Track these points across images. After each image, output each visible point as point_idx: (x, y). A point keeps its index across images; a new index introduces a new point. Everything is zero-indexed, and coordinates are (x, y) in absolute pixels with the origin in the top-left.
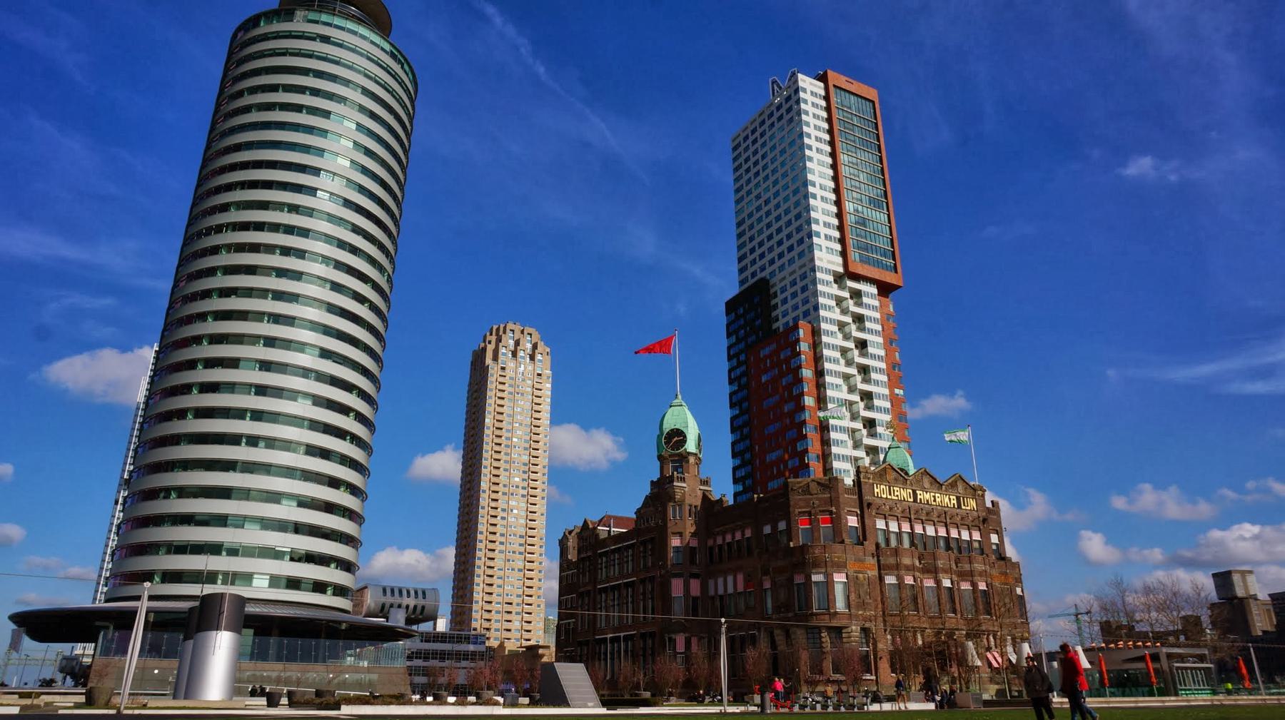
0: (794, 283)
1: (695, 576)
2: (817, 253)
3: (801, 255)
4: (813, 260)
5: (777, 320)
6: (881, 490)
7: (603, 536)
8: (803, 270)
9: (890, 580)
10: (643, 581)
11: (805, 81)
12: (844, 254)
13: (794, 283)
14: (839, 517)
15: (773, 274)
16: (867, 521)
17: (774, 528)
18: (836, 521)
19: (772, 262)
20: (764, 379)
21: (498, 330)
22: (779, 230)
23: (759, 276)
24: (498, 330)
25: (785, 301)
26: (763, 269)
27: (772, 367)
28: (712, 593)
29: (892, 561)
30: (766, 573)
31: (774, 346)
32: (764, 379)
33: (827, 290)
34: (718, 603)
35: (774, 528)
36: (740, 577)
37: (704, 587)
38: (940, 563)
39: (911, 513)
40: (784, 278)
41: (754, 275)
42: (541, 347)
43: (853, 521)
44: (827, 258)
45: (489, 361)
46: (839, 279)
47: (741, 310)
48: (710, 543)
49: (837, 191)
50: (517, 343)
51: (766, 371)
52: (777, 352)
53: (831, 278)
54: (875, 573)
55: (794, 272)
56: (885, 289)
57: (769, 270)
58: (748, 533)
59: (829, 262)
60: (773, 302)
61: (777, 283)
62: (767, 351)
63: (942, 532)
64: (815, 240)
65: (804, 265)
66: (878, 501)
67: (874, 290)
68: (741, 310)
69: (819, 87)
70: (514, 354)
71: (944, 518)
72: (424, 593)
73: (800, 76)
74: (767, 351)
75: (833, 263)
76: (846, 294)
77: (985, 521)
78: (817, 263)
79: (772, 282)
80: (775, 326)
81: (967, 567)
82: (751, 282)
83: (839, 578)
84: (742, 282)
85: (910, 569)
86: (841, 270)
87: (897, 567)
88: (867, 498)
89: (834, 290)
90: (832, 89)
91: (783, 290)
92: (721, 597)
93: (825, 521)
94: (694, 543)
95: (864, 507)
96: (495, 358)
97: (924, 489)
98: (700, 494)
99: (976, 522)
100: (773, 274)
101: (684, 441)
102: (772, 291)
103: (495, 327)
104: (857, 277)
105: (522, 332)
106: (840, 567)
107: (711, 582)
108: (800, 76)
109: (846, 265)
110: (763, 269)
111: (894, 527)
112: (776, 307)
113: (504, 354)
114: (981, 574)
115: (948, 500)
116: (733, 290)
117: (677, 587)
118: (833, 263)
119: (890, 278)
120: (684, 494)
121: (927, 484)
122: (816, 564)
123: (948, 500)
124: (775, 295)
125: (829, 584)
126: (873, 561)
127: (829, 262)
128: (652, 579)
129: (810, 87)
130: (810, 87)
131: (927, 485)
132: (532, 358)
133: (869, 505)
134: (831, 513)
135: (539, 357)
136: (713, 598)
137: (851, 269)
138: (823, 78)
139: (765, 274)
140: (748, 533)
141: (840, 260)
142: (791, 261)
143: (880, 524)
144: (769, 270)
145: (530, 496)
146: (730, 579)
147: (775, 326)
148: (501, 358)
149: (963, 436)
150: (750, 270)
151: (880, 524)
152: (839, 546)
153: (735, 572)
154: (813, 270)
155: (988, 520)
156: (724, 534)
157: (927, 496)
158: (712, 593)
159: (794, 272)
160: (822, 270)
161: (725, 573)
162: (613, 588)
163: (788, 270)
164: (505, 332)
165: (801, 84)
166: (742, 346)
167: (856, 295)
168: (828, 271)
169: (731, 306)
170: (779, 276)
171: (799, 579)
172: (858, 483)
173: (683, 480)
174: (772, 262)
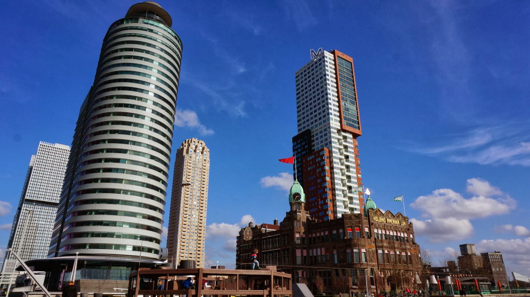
0: (321, 132)
1: (305, 248)
2: (331, 121)
3: (324, 121)
4: (329, 124)
5: (314, 146)
6: (375, 218)
7: (264, 232)
8: (325, 128)
9: (380, 251)
10: (284, 250)
11: (327, 54)
12: (341, 122)
13: (321, 132)
14: (362, 227)
17: (338, 231)
18: (361, 230)
19: (312, 123)
20: (309, 169)
21: (188, 141)
22: (315, 111)
23: (307, 128)
24: (188, 141)
25: (317, 139)
26: (308, 126)
27: (312, 165)
28: (311, 255)
29: (380, 244)
30: (334, 248)
31: (313, 156)
32: (309, 169)
33: (335, 136)
34: (313, 259)
35: (338, 231)
36: (323, 250)
37: (308, 253)
38: (396, 245)
39: (385, 227)
40: (317, 130)
41: (304, 127)
42: (206, 149)
43: (367, 230)
44: (335, 123)
45: (184, 154)
46: (339, 131)
47: (299, 141)
48: (310, 236)
49: (338, 97)
50: (196, 147)
51: (310, 166)
52: (314, 159)
53: (336, 131)
54: (374, 249)
55: (321, 128)
56: (355, 136)
57: (311, 126)
58: (327, 233)
59: (336, 125)
60: (312, 139)
61: (314, 132)
62: (311, 158)
63: (395, 234)
64: (330, 116)
65: (326, 125)
66: (375, 222)
67: (351, 136)
68: (299, 141)
69: (331, 56)
70: (195, 151)
71: (396, 229)
72: (162, 250)
73: (325, 51)
74: (311, 158)
75: (337, 125)
76: (341, 138)
77: (408, 230)
78: (331, 125)
79: (312, 131)
80: (313, 148)
81: (404, 247)
82: (303, 130)
83: (363, 250)
84: (299, 130)
85: (387, 247)
86: (339, 128)
87: (382, 247)
88: (371, 221)
89: (337, 136)
90: (336, 57)
91: (317, 134)
92: (315, 257)
93: (357, 230)
94: (304, 236)
95: (370, 225)
96: (187, 152)
97: (389, 218)
98: (306, 217)
100: (312, 128)
101: (300, 198)
102: (312, 134)
103: (187, 140)
104: (345, 131)
105: (198, 142)
106: (364, 246)
107: (311, 251)
108: (325, 51)
109: (341, 126)
110: (308, 126)
111: (380, 232)
112: (313, 141)
113: (191, 151)
115: (397, 222)
116: (296, 133)
117: (298, 253)
118: (337, 125)
119: (357, 131)
120: (300, 218)
121: (390, 216)
122: (355, 246)
123: (397, 222)
124: (313, 136)
125: (360, 253)
126: (373, 244)
127: (336, 125)
128: (288, 250)
129: (328, 56)
130: (328, 56)
131: (390, 216)
132: (202, 153)
133: (372, 224)
134: (359, 227)
135: (205, 153)
136: (311, 257)
137: (344, 128)
138: (333, 53)
139: (309, 128)
140: (327, 233)
141: (339, 124)
142: (320, 124)
143: (376, 231)
144: (311, 126)
145: (200, 210)
146: (319, 250)
147: (313, 148)
148: (190, 153)
149: (400, 199)
150: (303, 126)
151: (376, 231)
152: (363, 239)
153: (321, 248)
154: (330, 128)
155: (409, 229)
156: (316, 233)
157: (390, 220)
158: (311, 255)
159: (321, 128)
160: (333, 128)
161: (316, 248)
162: (269, 252)
163: (319, 127)
164: (191, 142)
165: (325, 55)
166: (300, 155)
167: (345, 138)
168: (335, 128)
169: (295, 139)
170: (315, 129)
171: (348, 251)
173: (300, 212)
174: (312, 123)
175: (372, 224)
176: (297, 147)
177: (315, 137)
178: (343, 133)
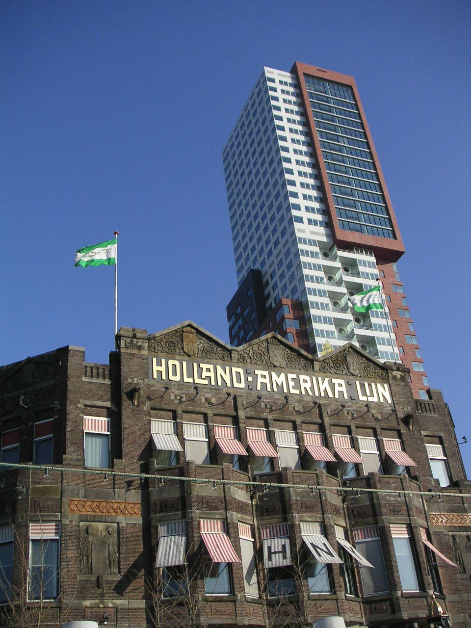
2: (297, 225)
3: (283, 233)
4: (293, 233)
11: (270, 72)
12: (329, 224)
15: (263, 264)
16: (126, 422)
26: (255, 261)
33: (313, 264)
44: (309, 231)
47: (239, 310)
56: (385, 257)
57: (260, 260)
59: (312, 233)
67: (373, 259)
68: (239, 310)
71: (320, 417)
77: (407, 420)
78: (298, 234)
88: (130, 379)
90: (302, 79)
99: (394, 424)
100: (263, 264)
102: (264, 281)
109: (332, 234)
110: (255, 261)
112: (268, 296)
114: (394, 510)
119: (387, 244)
127: (312, 233)
130: (278, 78)
133: (132, 394)
160: (304, 241)
165: (268, 75)
168: (312, 242)
170: (268, 262)
172: (115, 358)
175: (132, 394)
176: (236, 328)
177: (271, 283)
178: (341, 253)
